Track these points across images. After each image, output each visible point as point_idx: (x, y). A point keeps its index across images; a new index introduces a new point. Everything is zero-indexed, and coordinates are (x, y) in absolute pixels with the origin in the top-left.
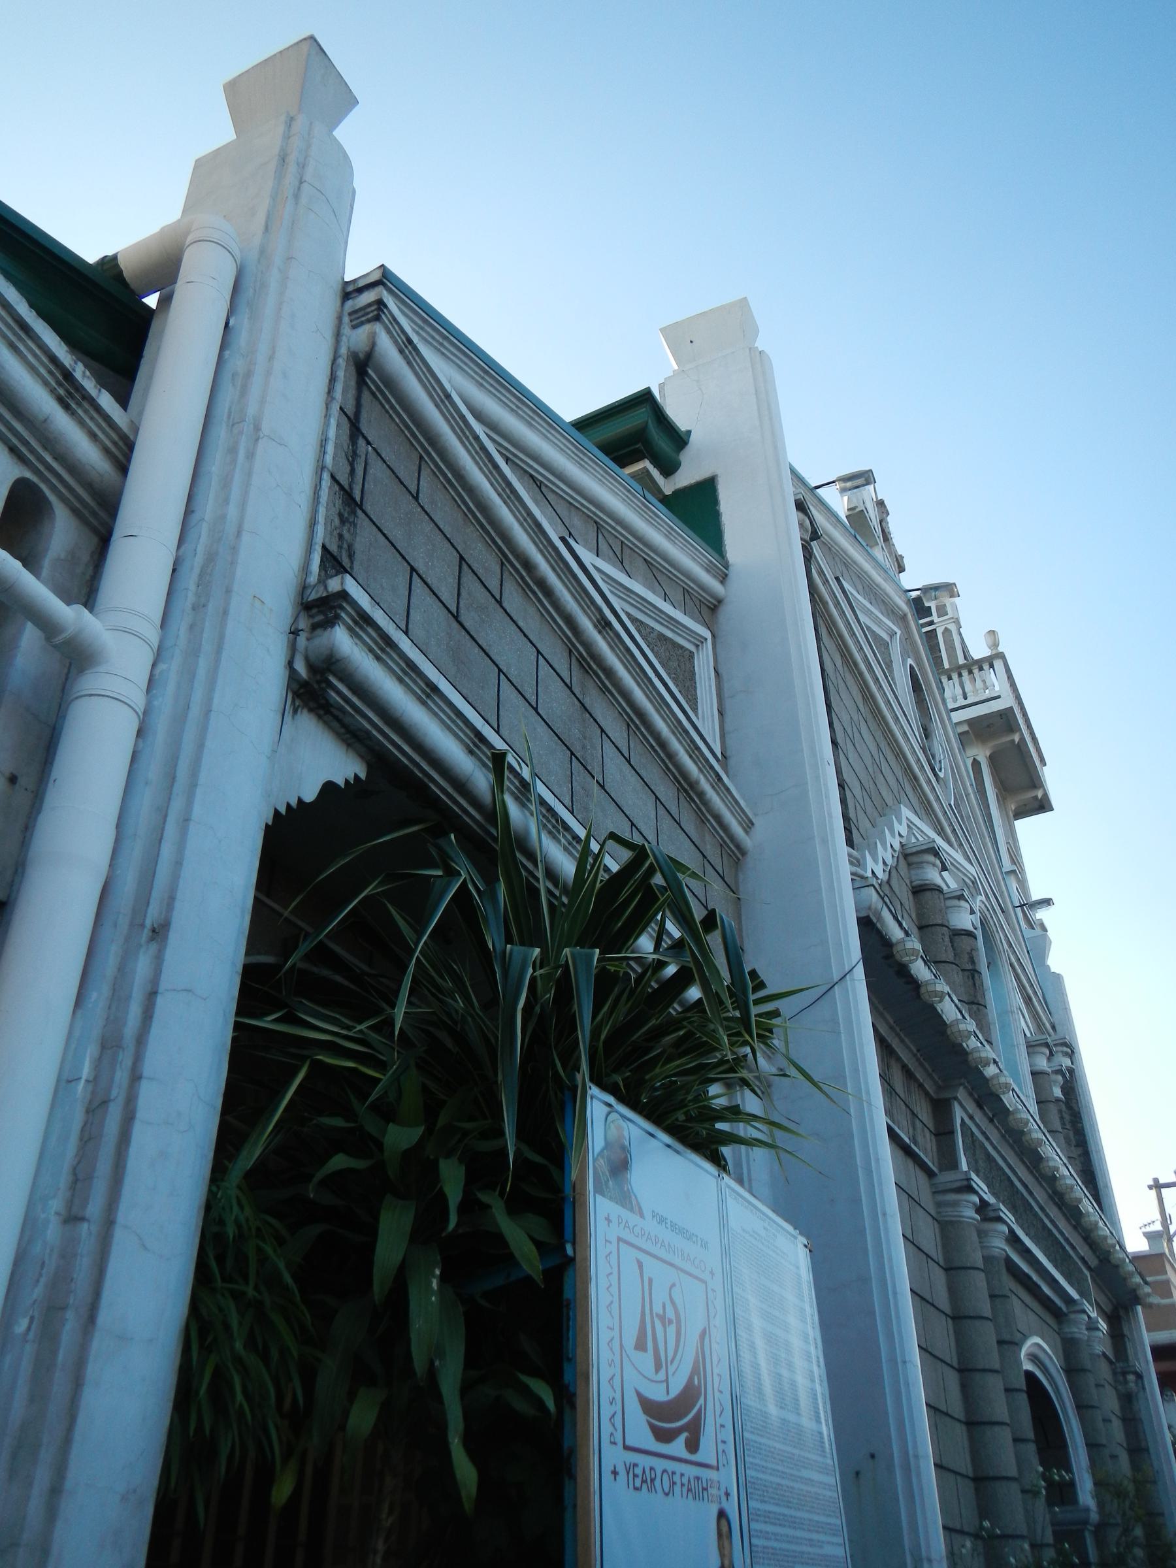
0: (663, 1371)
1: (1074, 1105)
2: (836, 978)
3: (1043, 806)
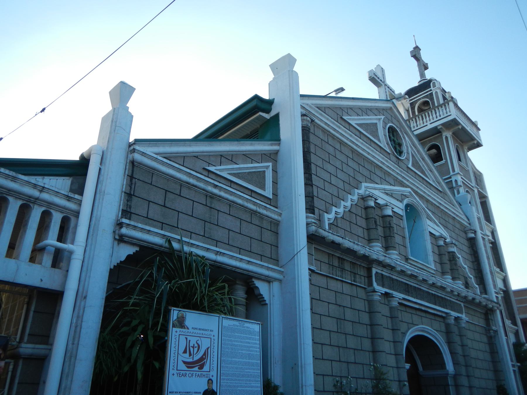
0: (192, 357)
1: (474, 248)
2: (296, 253)
3: (479, 145)
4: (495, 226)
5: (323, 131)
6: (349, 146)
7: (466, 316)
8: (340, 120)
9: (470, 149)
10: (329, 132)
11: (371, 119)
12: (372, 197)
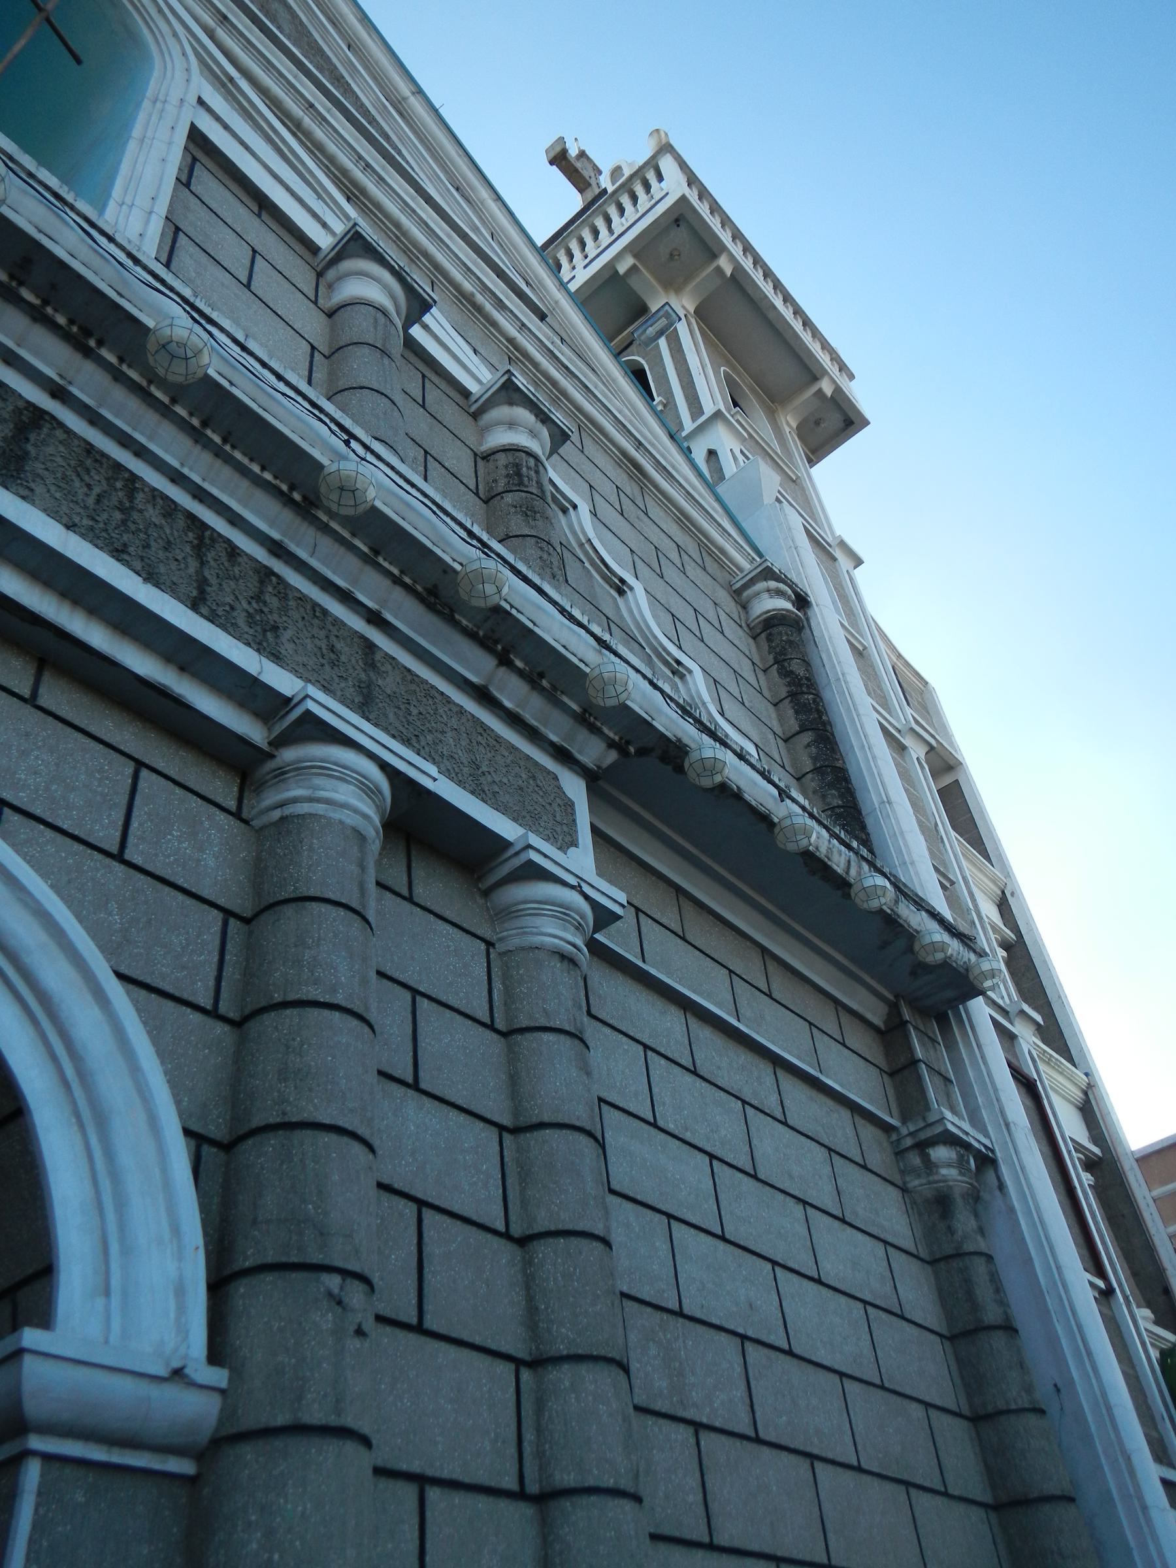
4: (1008, 873)
9: (816, 451)
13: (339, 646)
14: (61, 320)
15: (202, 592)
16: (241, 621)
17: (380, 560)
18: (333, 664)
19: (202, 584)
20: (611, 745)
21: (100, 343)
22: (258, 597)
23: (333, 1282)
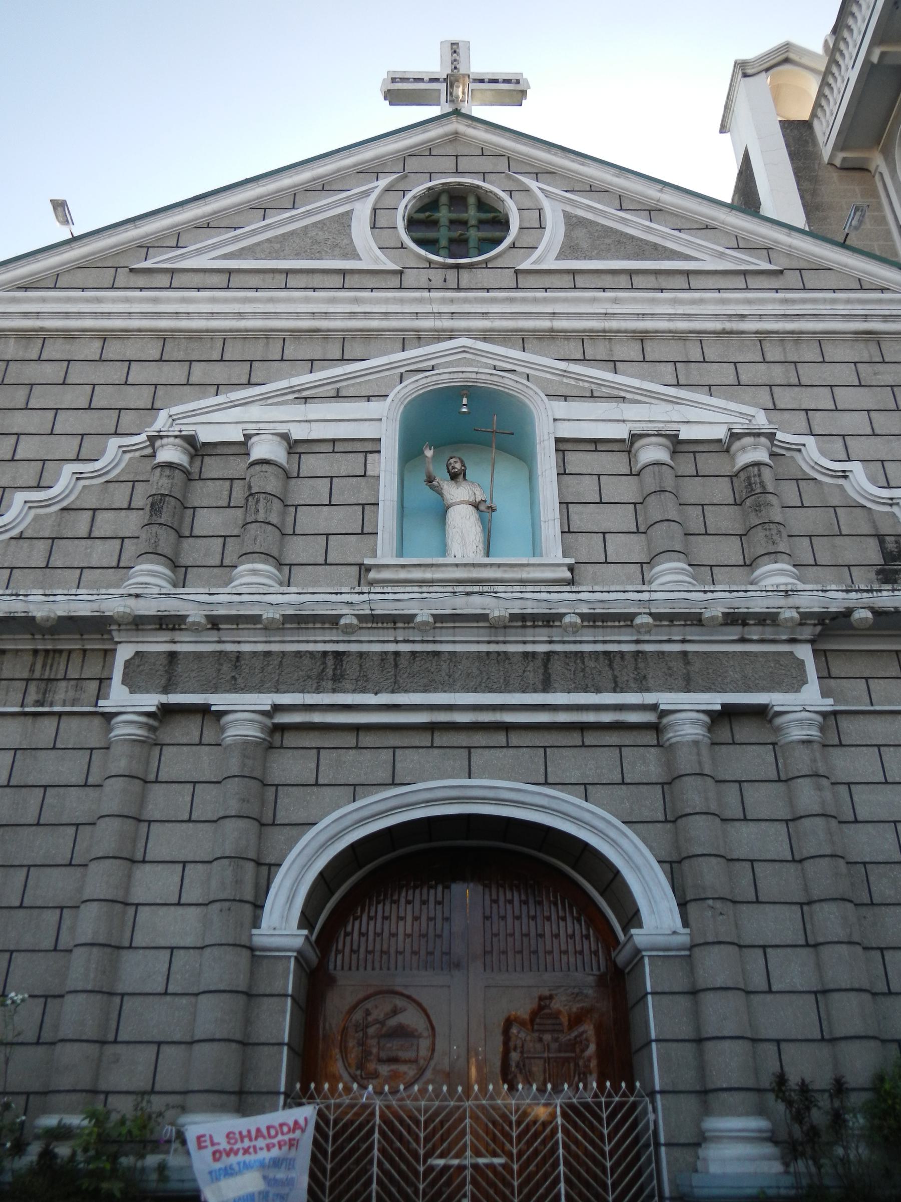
5: (19, 338)
6: (140, 330)
7: (824, 695)
8: (123, 278)
10: (42, 329)
11: (309, 213)
12: (161, 437)
13: (671, 664)
14: (540, 623)
15: (616, 682)
16: (632, 685)
17: (675, 623)
18: (671, 675)
19: (615, 678)
20: (815, 625)
21: (553, 622)
22: (636, 669)
23: (710, 902)
